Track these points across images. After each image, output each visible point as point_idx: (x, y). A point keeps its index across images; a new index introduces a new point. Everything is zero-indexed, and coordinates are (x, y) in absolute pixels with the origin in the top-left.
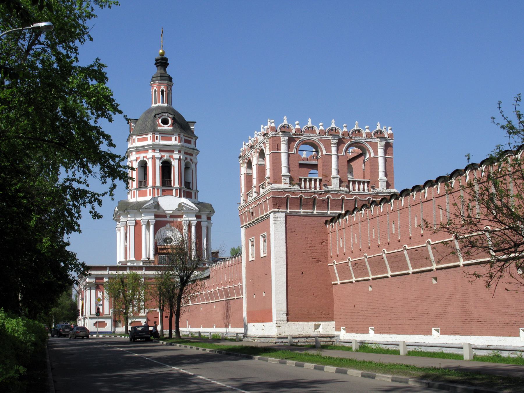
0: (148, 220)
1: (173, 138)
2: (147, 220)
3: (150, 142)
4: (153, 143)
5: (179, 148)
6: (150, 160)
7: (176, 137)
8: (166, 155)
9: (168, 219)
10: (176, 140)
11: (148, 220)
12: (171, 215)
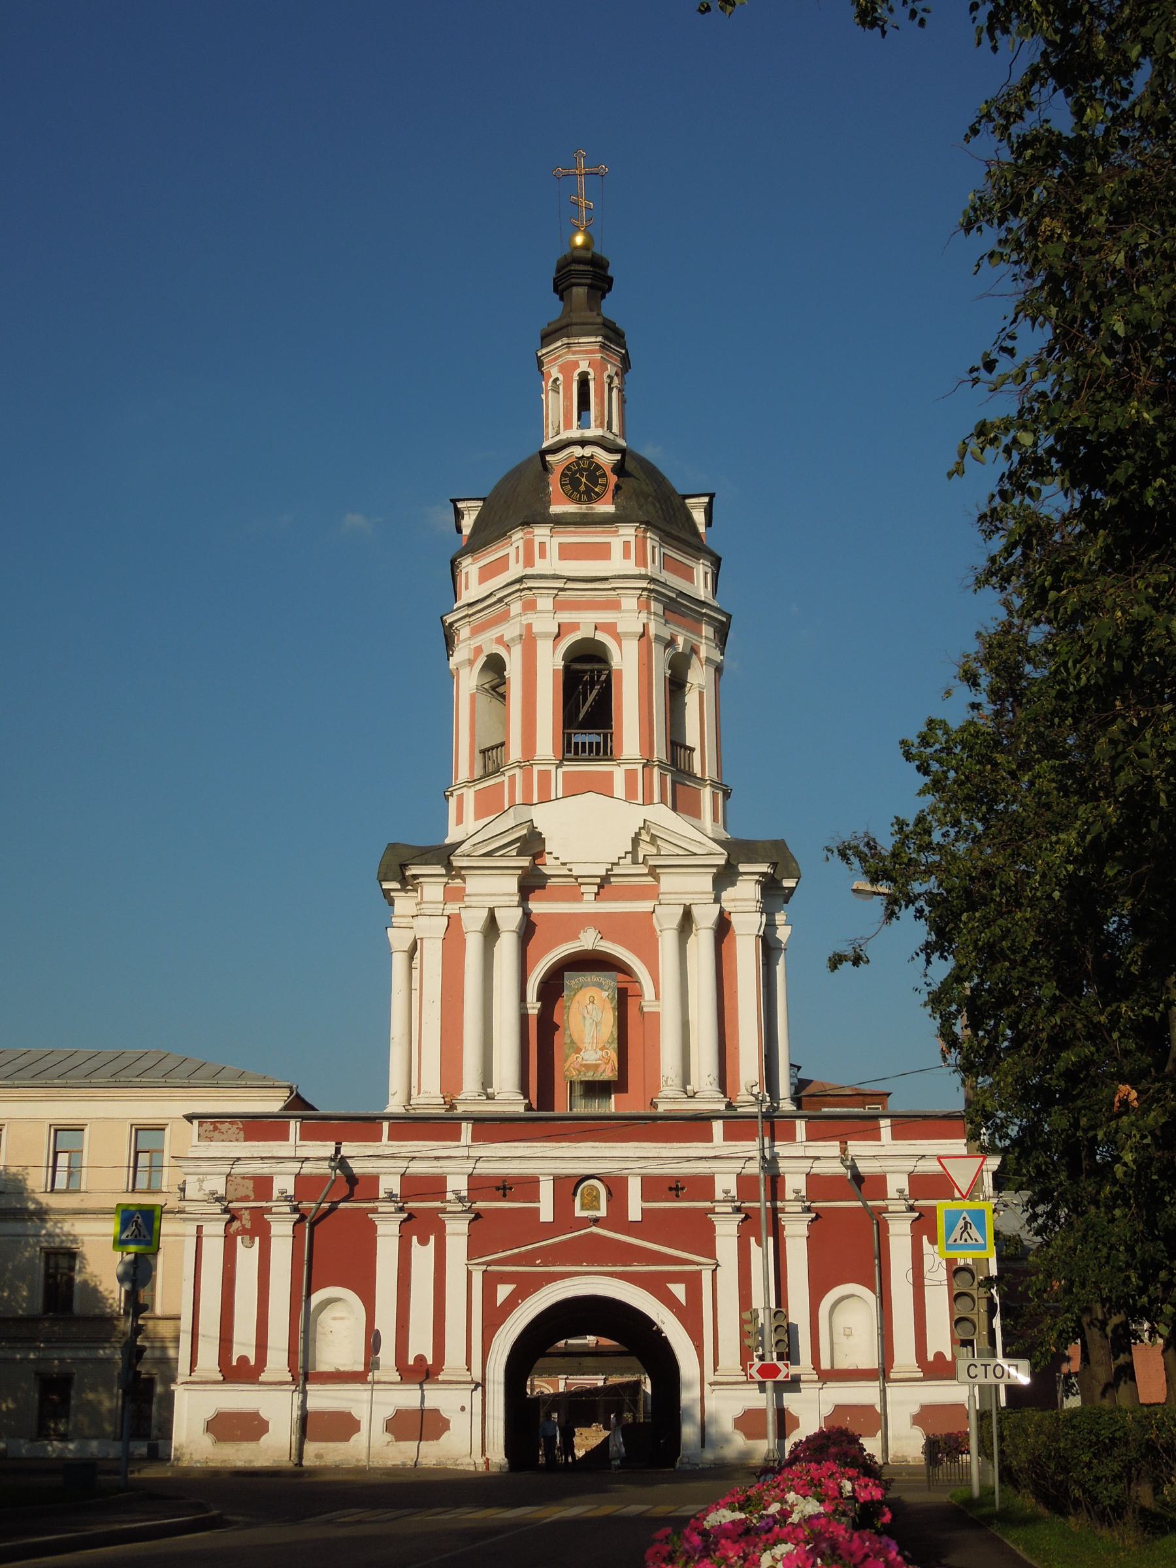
0: (492, 911)
1: (616, 544)
2: (485, 913)
3: (516, 570)
4: (529, 571)
5: (644, 589)
6: (517, 652)
7: (627, 544)
8: (586, 623)
9: (589, 905)
10: (626, 555)
11: (492, 911)
12: (600, 886)
